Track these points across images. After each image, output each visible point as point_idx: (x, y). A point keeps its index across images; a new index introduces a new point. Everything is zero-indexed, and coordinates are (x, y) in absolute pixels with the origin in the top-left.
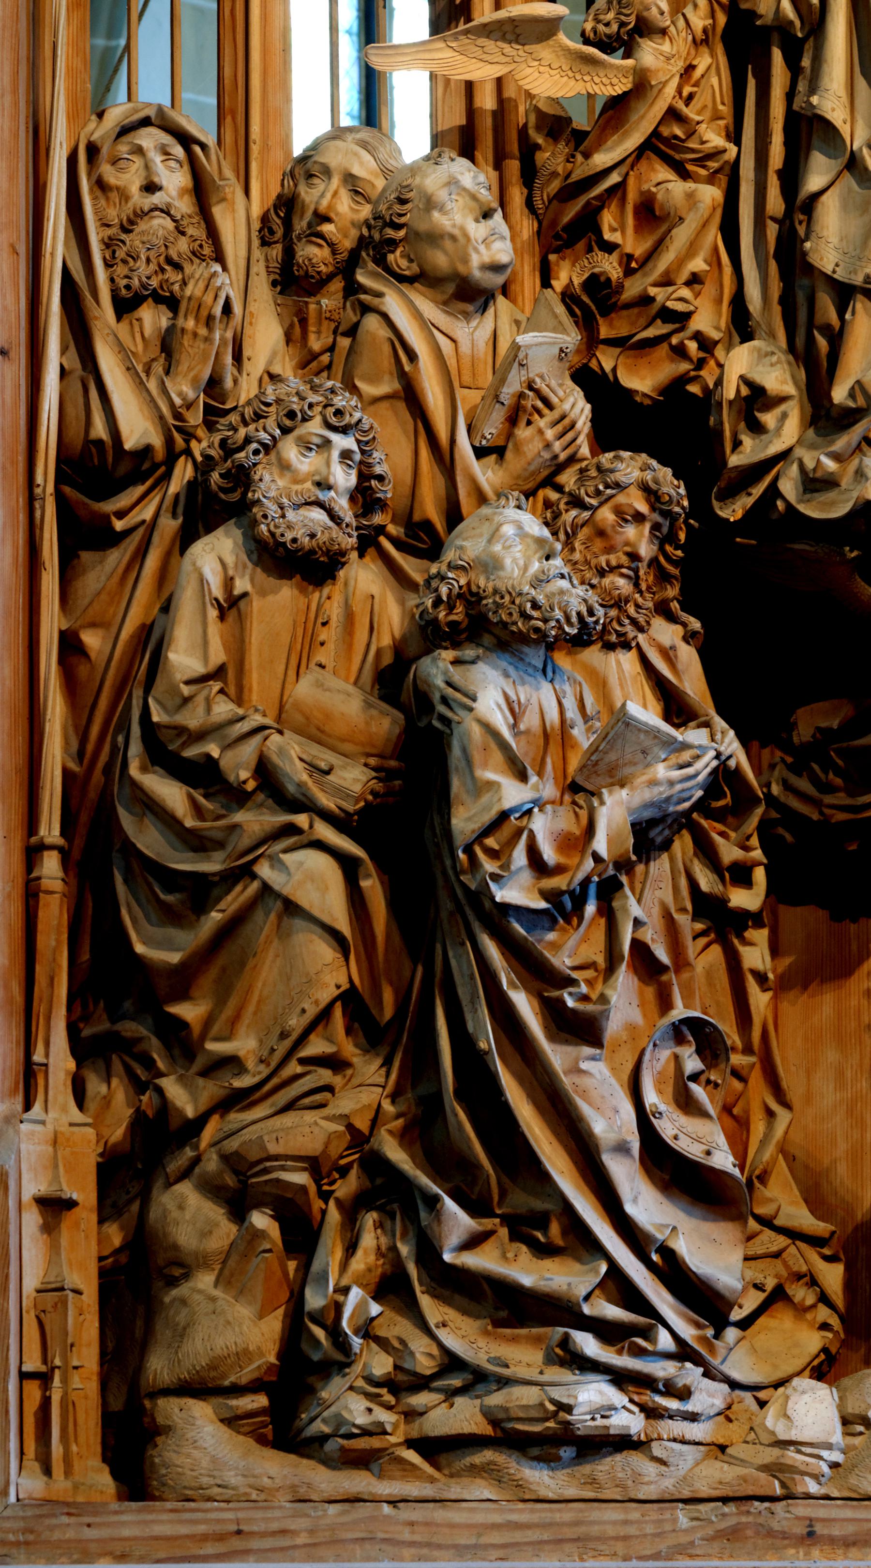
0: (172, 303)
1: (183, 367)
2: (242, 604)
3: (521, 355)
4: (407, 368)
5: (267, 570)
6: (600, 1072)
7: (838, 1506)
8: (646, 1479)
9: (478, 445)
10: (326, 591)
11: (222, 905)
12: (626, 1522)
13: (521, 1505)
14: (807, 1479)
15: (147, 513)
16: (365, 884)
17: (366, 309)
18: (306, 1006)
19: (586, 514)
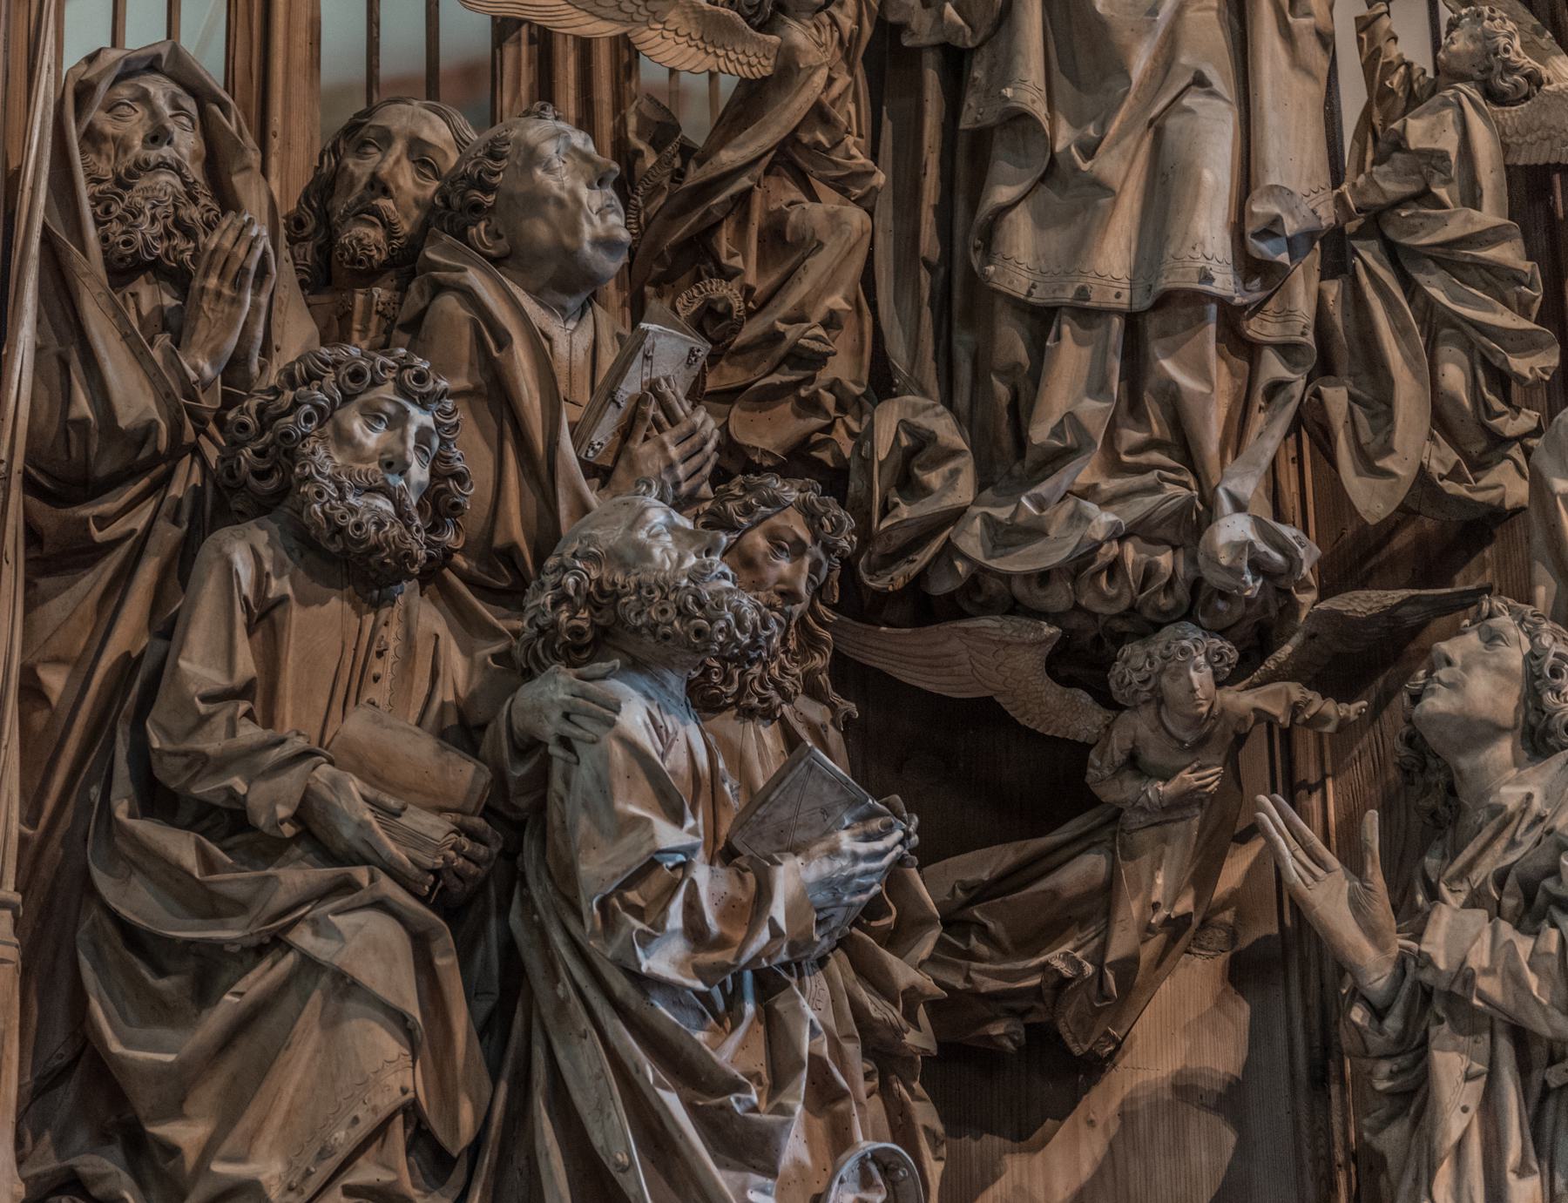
0: (179, 278)
1: (200, 336)
3: (648, 343)
4: (495, 354)
5: (310, 573)
10: (384, 613)
11: (239, 987)
15: (139, 520)
16: (440, 962)
17: (439, 288)
18: (360, 1114)
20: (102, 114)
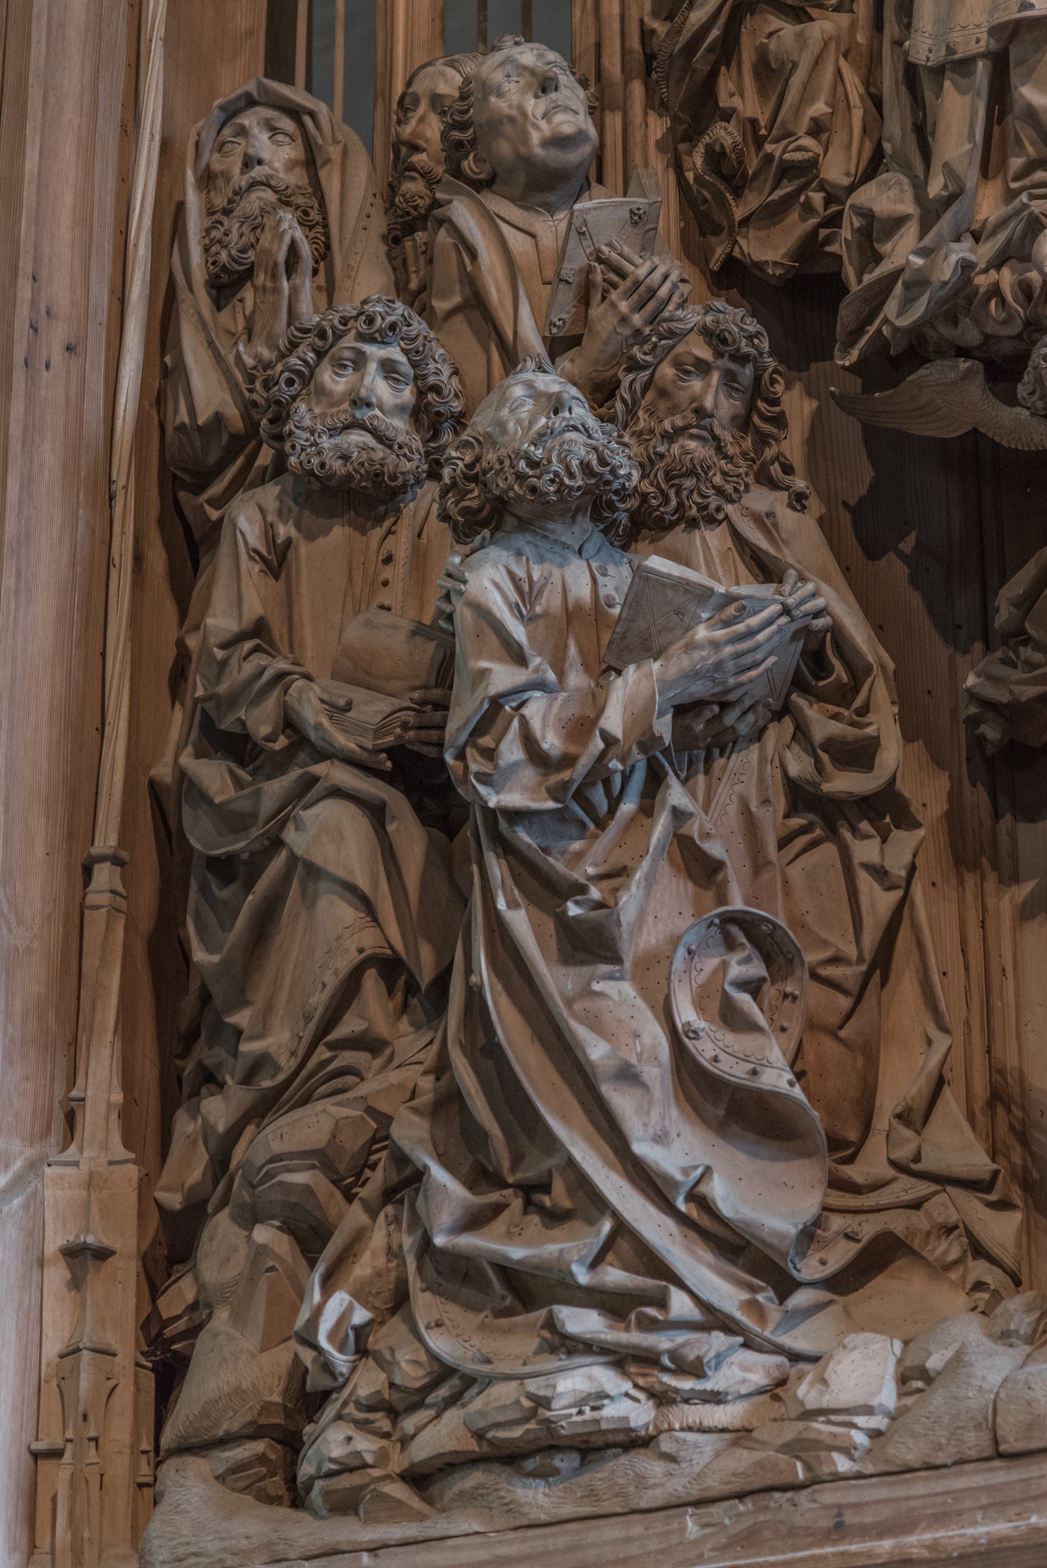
2: (291, 555)
4: (469, 268)
6: (619, 992)
7: (871, 1485)
8: (651, 1481)
9: (547, 334)
12: (627, 1540)
13: (511, 1535)
14: (836, 1455)
19: (644, 375)
20: (216, 156)
